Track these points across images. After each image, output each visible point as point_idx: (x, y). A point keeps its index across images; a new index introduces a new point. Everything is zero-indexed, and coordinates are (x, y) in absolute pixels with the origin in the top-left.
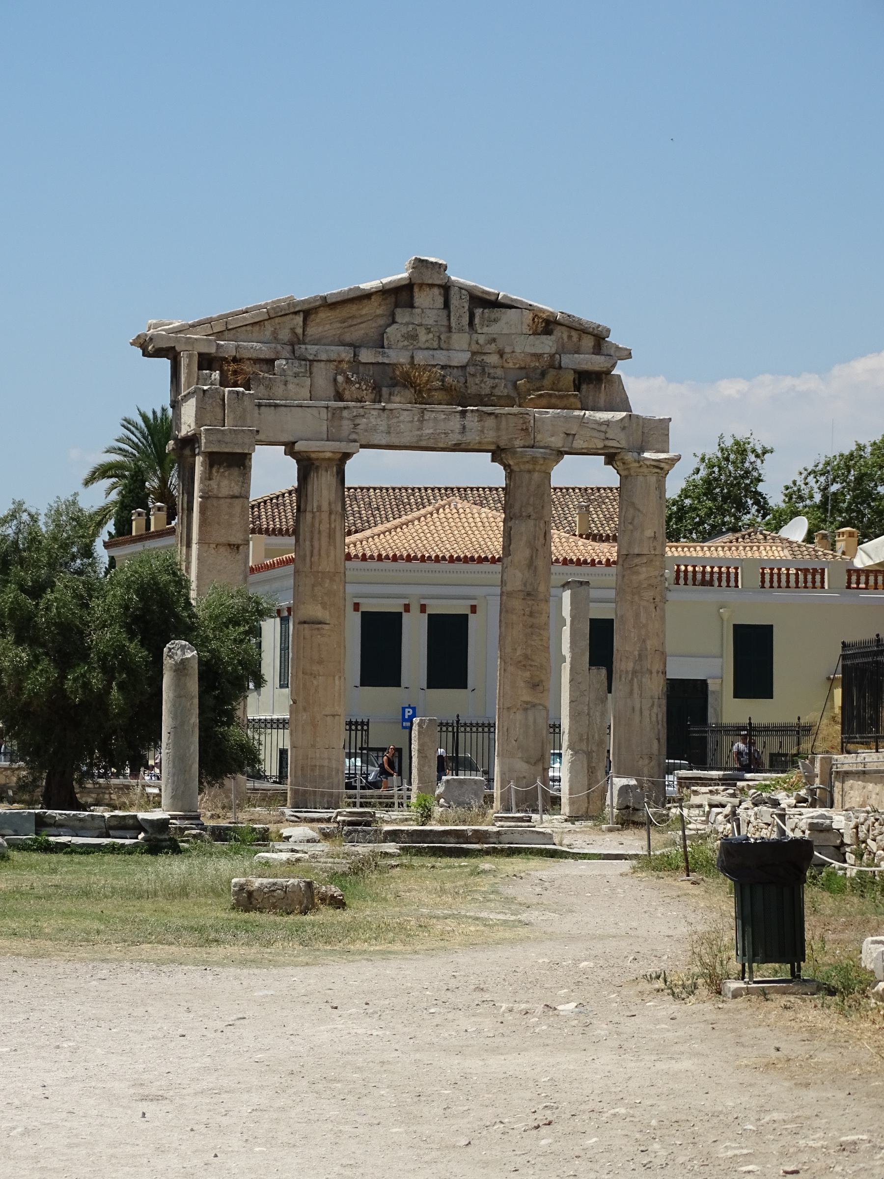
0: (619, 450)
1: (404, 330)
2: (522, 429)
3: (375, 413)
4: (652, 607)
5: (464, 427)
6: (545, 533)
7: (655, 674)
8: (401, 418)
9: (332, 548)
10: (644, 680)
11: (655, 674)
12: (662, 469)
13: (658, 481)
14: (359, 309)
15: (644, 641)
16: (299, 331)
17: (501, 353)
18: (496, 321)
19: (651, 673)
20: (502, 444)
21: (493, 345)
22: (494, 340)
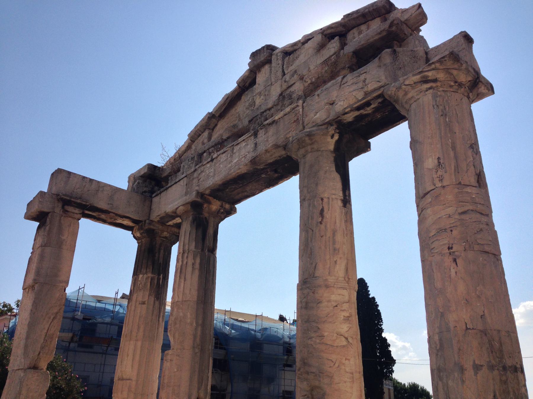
0: (382, 89)
1: (247, 104)
2: (295, 121)
3: (208, 165)
4: (448, 261)
5: (256, 144)
6: (322, 211)
7: (470, 373)
8: (222, 160)
9: (182, 281)
10: (450, 383)
11: (470, 373)
12: (435, 81)
13: (435, 96)
14: (236, 109)
15: (442, 315)
16: (206, 141)
17: (302, 78)
18: (297, 58)
19: (462, 370)
20: (280, 142)
21: (295, 76)
22: (296, 72)
